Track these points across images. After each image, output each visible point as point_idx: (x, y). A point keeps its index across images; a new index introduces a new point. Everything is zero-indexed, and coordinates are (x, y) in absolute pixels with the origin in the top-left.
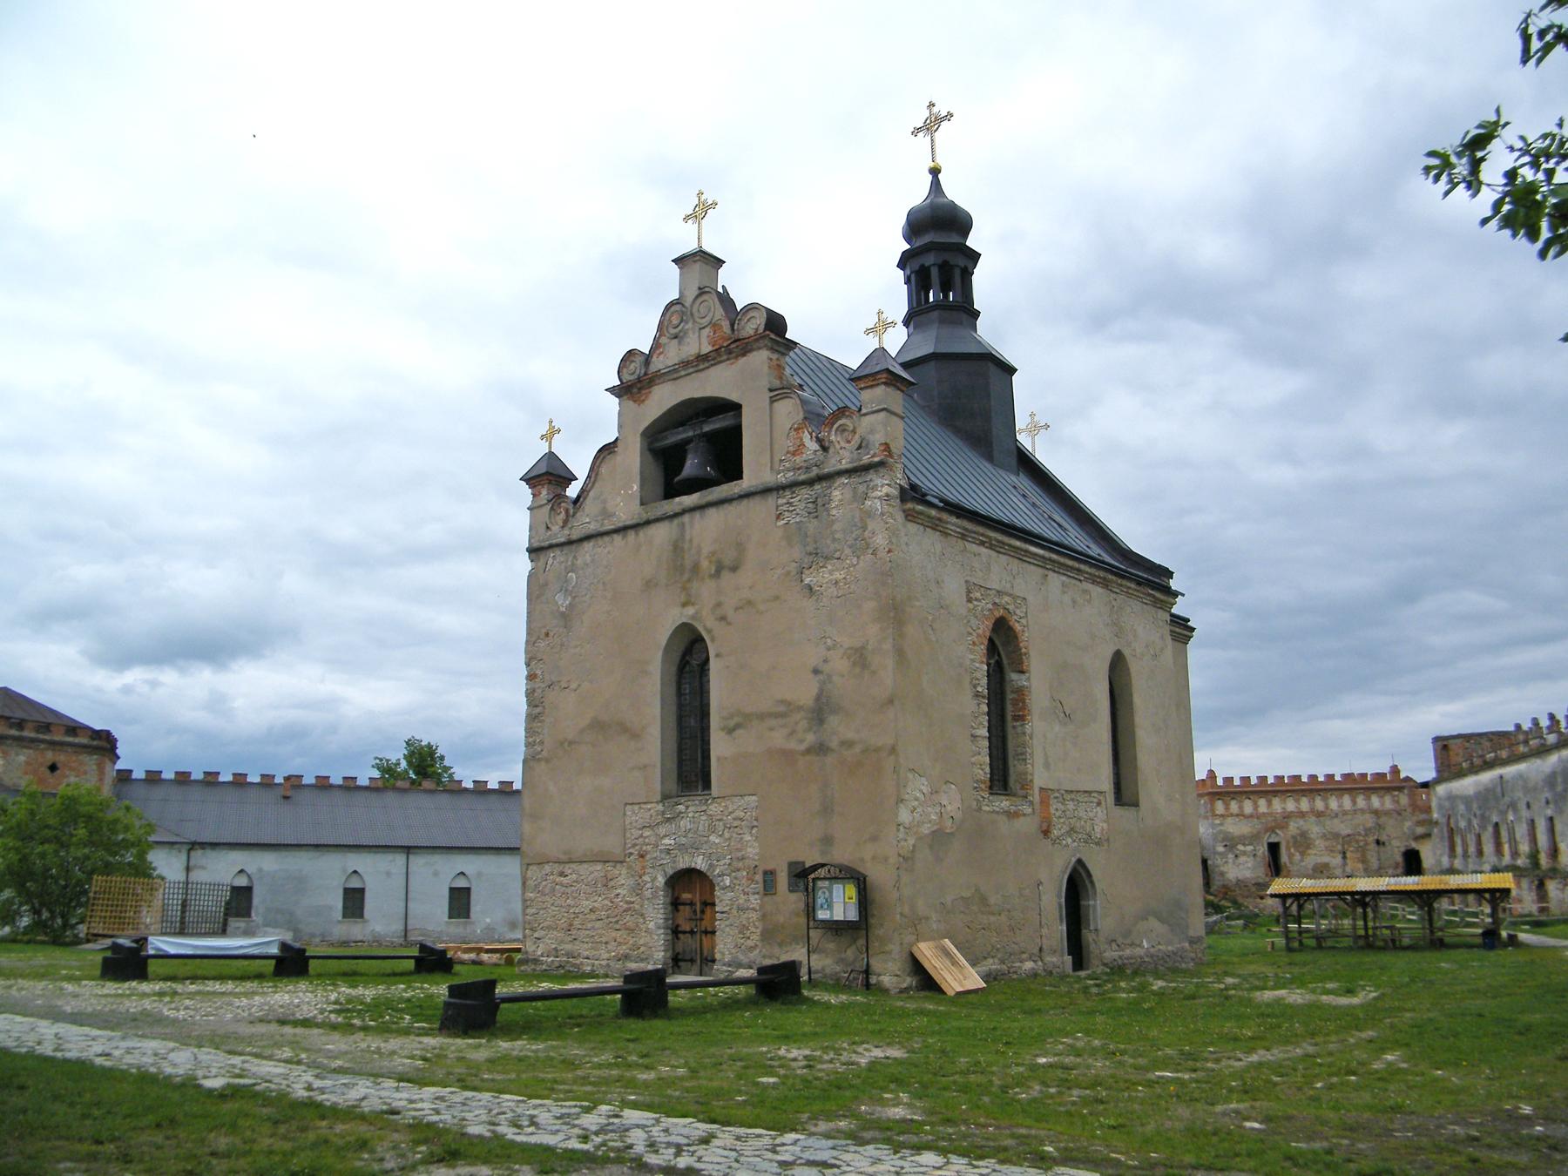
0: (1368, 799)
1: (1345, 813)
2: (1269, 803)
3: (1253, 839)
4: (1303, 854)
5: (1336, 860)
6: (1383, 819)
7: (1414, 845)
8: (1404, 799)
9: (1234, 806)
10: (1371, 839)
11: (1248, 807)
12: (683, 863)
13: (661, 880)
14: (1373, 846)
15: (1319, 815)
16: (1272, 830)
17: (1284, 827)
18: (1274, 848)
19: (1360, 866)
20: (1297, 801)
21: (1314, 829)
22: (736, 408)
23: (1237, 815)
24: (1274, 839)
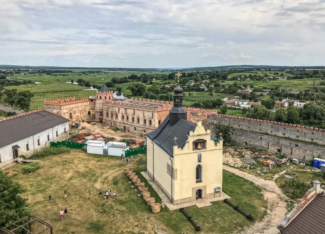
0: (84, 103)
1: (81, 106)
2: (70, 106)
3: (68, 113)
4: (75, 114)
5: (79, 115)
6: (86, 107)
7: (90, 110)
8: (88, 103)
9: (65, 107)
10: (84, 110)
11: (67, 106)
12: (198, 189)
13: (195, 191)
14: (84, 111)
15: (77, 107)
16: (70, 111)
17: (72, 110)
18: (71, 114)
19: (83, 115)
20: (74, 105)
21: (76, 110)
22: (206, 141)
23: (66, 109)
24: (70, 112)
